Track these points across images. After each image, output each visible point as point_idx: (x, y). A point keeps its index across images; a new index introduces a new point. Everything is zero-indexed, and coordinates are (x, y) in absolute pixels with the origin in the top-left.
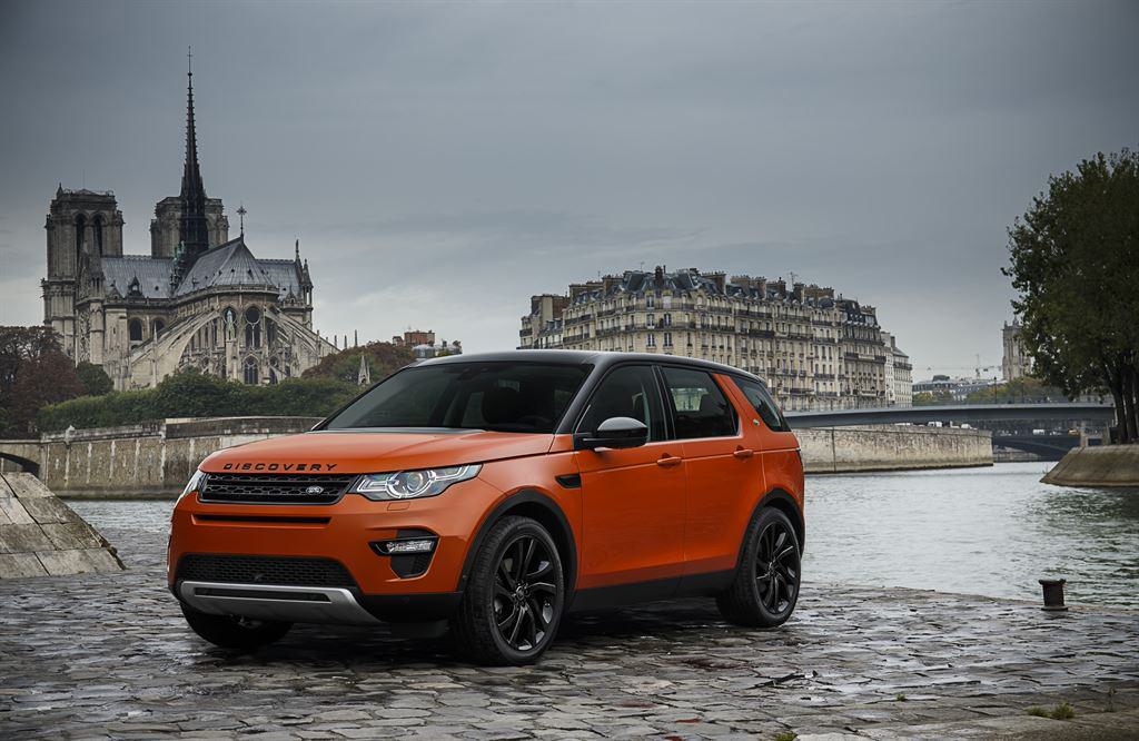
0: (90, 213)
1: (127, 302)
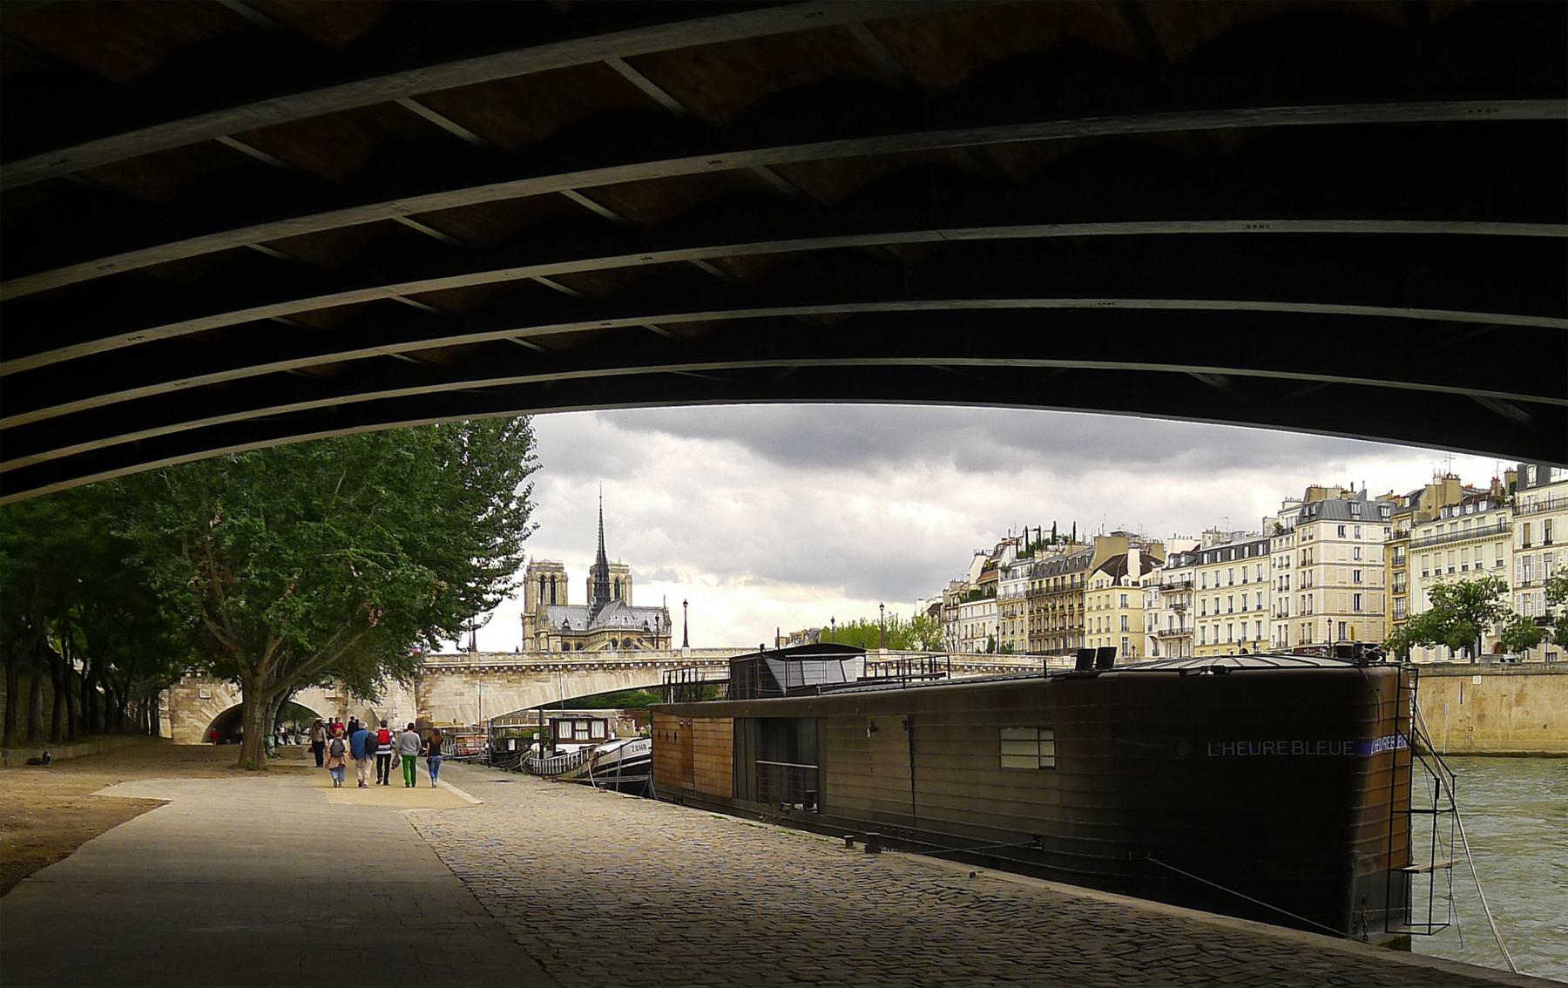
0: (548, 574)
1: (561, 633)
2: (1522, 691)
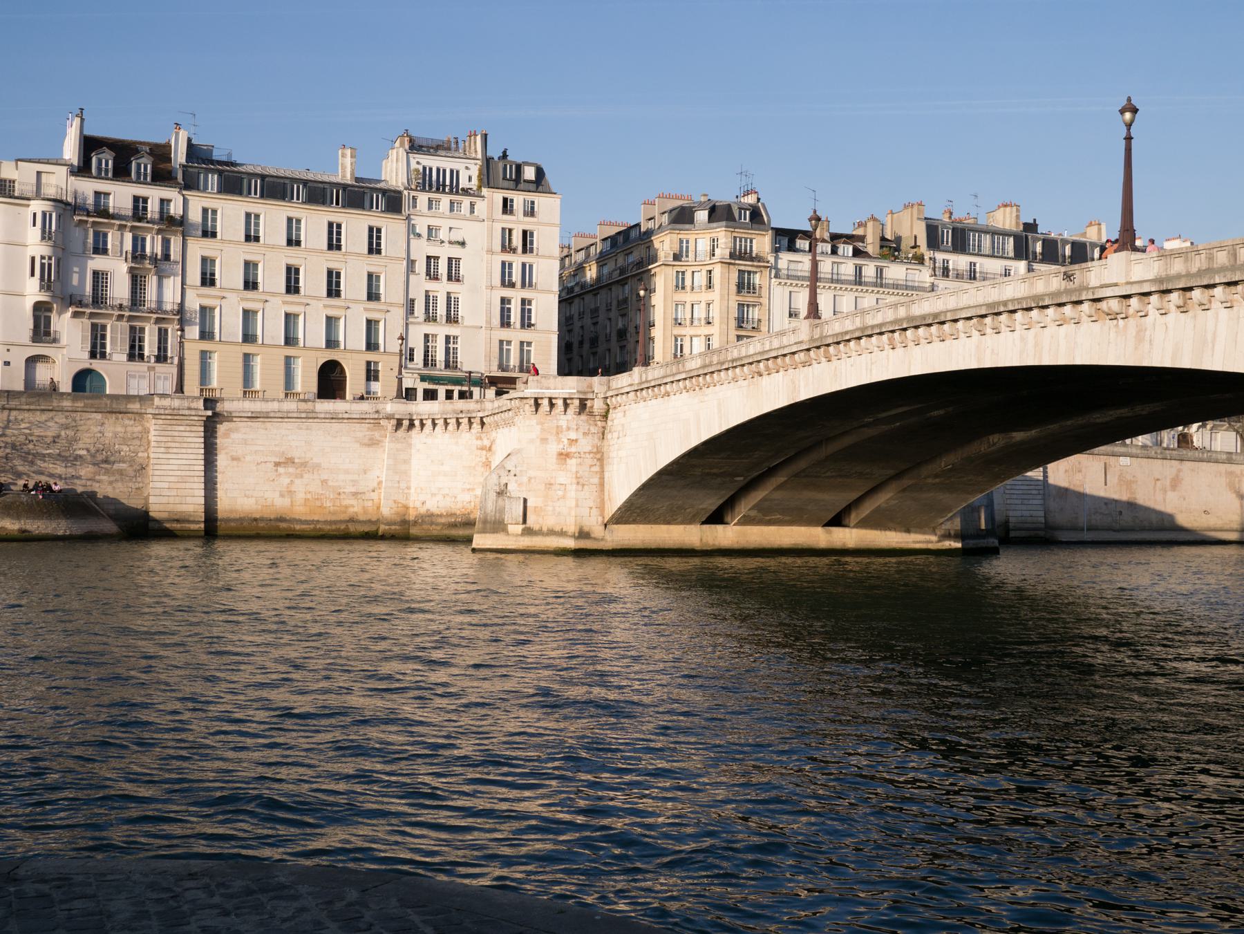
2: (1177, 476)
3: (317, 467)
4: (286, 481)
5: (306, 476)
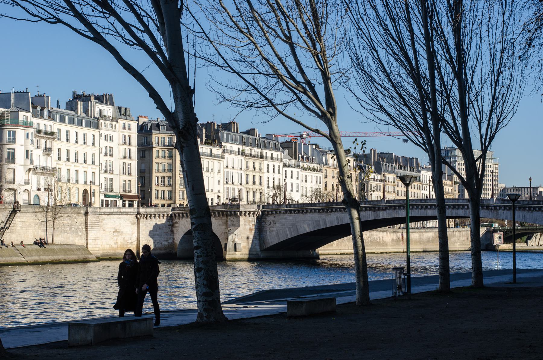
3: (122, 233)
4: (115, 238)
5: (120, 236)
